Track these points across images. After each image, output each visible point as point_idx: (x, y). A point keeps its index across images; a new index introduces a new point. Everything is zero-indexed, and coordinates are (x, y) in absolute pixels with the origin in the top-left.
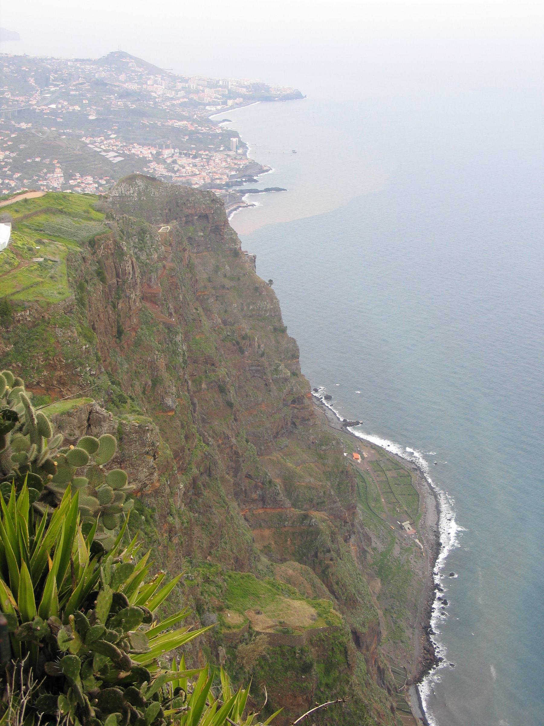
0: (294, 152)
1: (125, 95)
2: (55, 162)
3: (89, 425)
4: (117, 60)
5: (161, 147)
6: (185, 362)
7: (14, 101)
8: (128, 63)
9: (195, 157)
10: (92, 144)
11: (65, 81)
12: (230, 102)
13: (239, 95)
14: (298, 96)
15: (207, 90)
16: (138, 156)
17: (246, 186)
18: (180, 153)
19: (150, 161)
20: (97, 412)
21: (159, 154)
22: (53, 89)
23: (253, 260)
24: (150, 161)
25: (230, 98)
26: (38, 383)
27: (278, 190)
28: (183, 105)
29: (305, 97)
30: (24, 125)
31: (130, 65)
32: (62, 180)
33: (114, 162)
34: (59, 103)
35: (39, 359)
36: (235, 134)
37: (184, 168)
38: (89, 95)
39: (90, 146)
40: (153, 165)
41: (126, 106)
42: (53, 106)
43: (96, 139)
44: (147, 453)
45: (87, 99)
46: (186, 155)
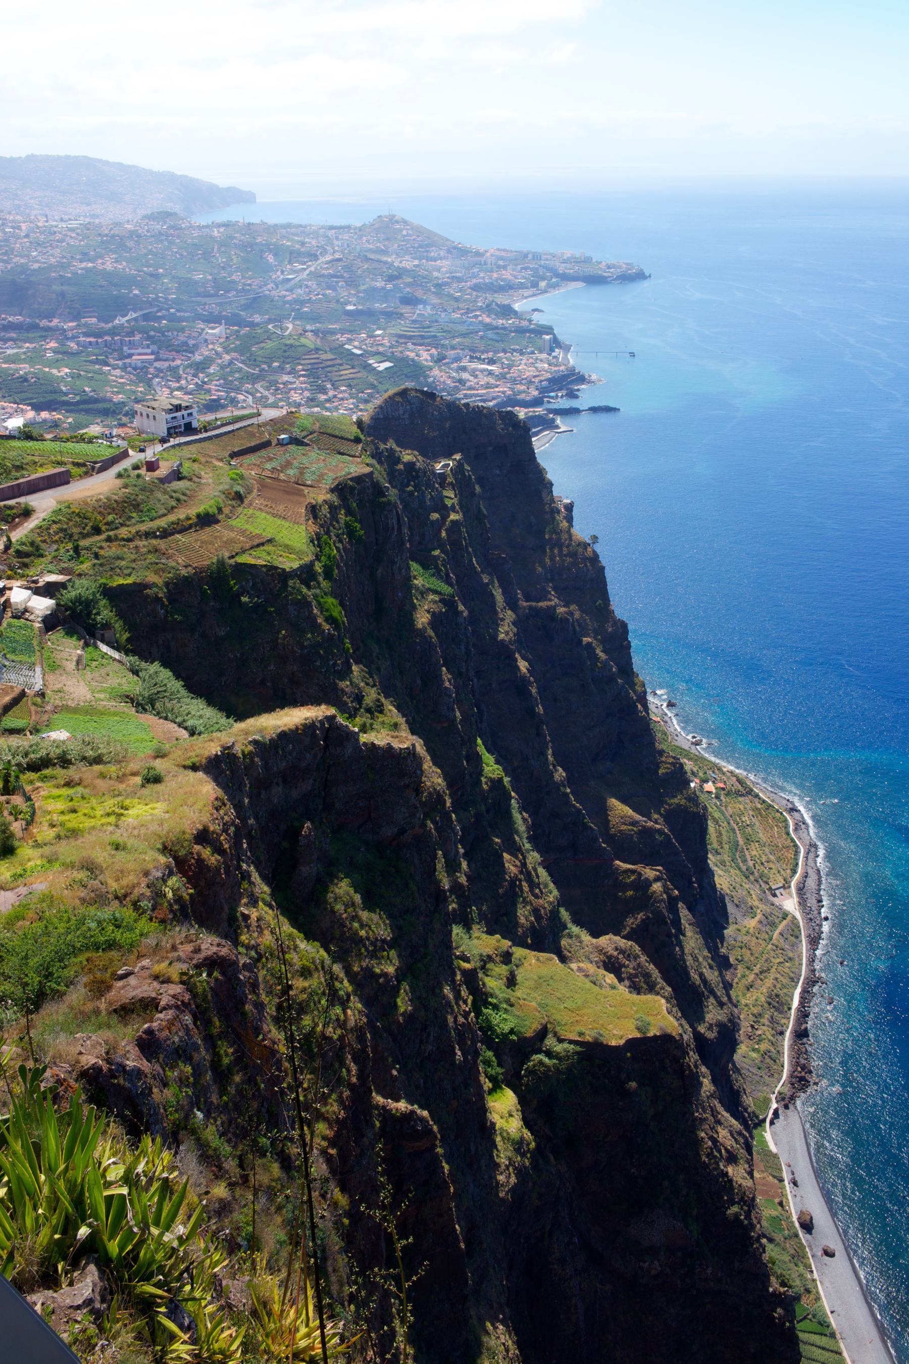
0: (632, 355)
3: (326, 746)
4: (388, 227)
6: (468, 652)
9: (491, 362)
12: (543, 284)
13: (557, 275)
14: (641, 276)
17: (564, 403)
18: (472, 357)
19: (431, 369)
20: (338, 728)
23: (569, 508)
25: (543, 279)
26: (263, 682)
27: (608, 409)
29: (650, 276)
32: (307, 394)
33: (380, 369)
35: (264, 648)
36: (549, 330)
37: (476, 377)
39: (347, 346)
44: (407, 786)
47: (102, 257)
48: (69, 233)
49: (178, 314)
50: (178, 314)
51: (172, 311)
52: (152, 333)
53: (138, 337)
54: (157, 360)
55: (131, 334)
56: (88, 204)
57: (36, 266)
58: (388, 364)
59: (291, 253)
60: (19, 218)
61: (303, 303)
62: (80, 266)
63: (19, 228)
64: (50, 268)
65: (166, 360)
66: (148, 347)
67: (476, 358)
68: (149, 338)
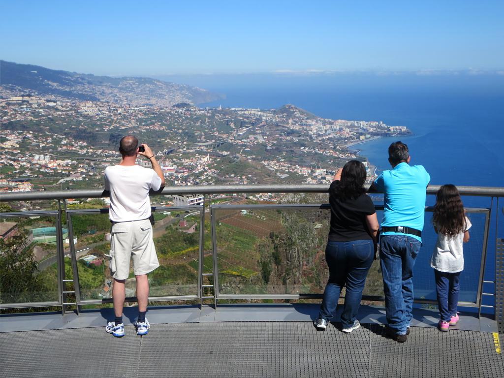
1: (291, 133)
2: (244, 177)
5: (314, 167)
7: (220, 137)
8: (294, 112)
10: (268, 165)
11: (253, 124)
15: (348, 130)
16: (298, 173)
18: (327, 172)
19: (307, 177)
21: (312, 172)
22: (245, 129)
24: (307, 177)
25: (362, 134)
28: (329, 139)
30: (225, 153)
31: (296, 113)
33: (283, 177)
34: (248, 138)
38: (268, 133)
39: (267, 166)
40: (309, 179)
41: (291, 140)
42: (245, 141)
43: (271, 162)
45: (267, 136)
46: (330, 173)
47: (153, 124)
48: (140, 113)
49: (187, 151)
50: (187, 151)
51: (185, 149)
52: (175, 160)
53: (167, 163)
54: (176, 172)
55: (164, 161)
56: (149, 100)
57: (123, 128)
58: (287, 175)
59: (241, 122)
60: (117, 105)
61: (246, 146)
62: (144, 129)
63: (117, 110)
64: (131, 129)
65: (180, 172)
66: (172, 166)
67: (329, 172)
68: (173, 162)
